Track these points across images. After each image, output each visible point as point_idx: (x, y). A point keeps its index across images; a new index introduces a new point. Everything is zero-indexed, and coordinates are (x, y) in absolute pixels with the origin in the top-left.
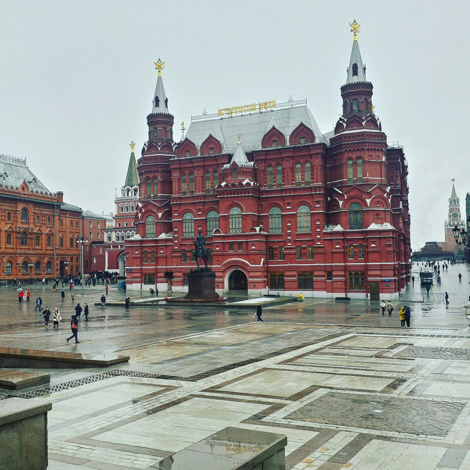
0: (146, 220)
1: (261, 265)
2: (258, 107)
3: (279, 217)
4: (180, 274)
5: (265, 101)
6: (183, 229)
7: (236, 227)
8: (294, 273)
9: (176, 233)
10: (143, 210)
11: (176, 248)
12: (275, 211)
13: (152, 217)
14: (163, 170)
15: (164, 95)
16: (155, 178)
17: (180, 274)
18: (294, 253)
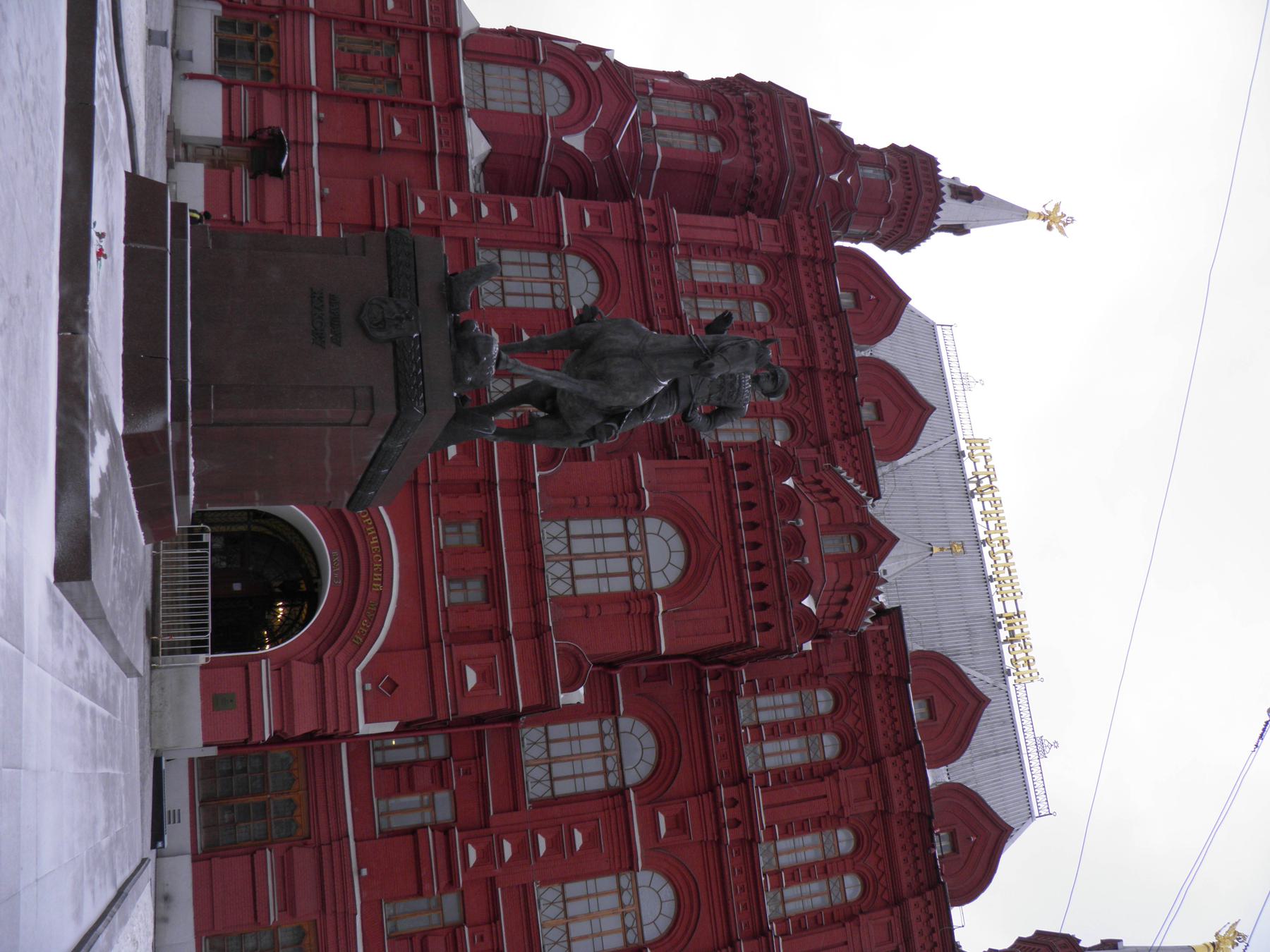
0: (550, 71)
1: (364, 728)
2: (1011, 609)
3: (606, 772)
4: (274, 212)
5: (1033, 639)
6: (514, 248)
7: (581, 557)
8: (306, 903)
9: (500, 211)
10: (594, 65)
11: (421, 207)
12: (639, 751)
13: (566, 101)
14: (757, 181)
15: (980, 223)
16: (727, 140)
17: (274, 212)
18: (426, 887)
